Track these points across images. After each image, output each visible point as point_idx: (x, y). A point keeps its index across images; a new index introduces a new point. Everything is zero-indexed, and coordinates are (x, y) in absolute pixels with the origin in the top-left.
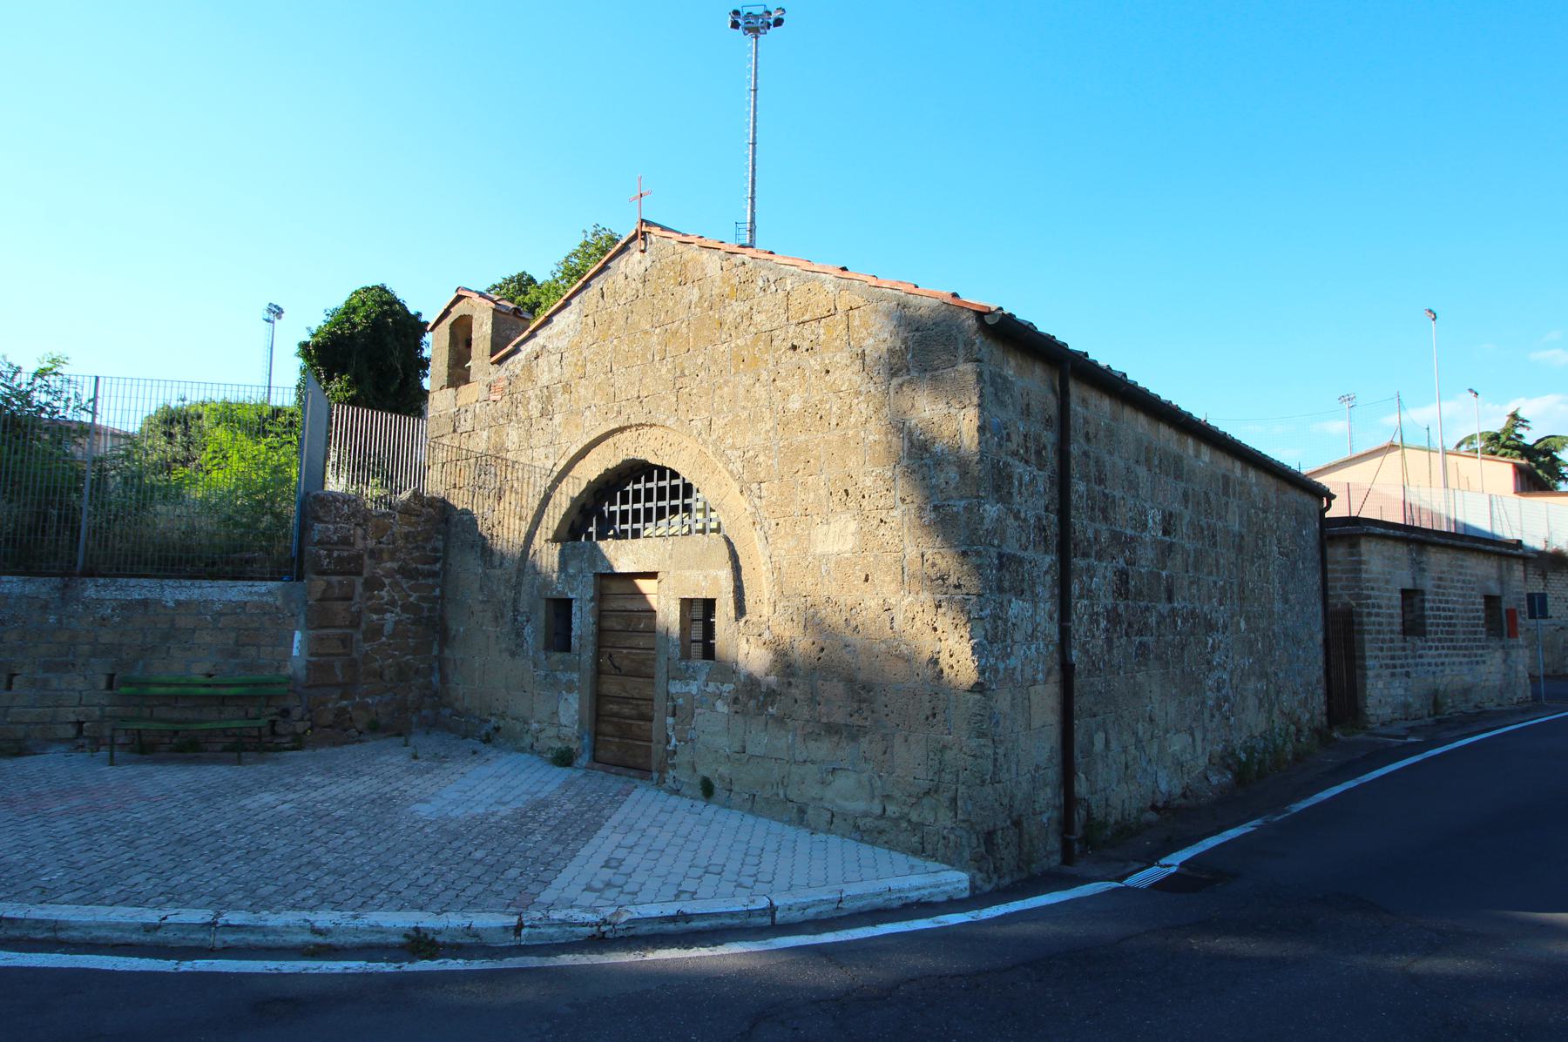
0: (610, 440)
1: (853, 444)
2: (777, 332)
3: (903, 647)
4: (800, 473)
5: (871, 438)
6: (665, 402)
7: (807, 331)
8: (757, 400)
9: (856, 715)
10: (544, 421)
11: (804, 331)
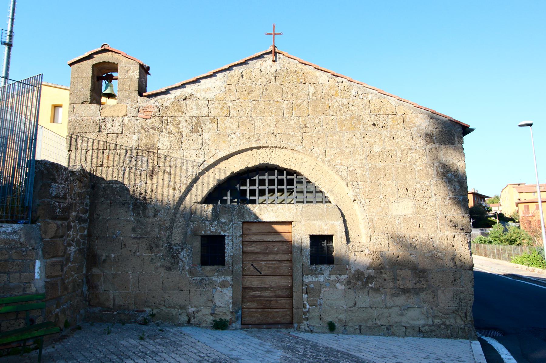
0: (249, 152)
1: (409, 170)
2: (365, 117)
3: (439, 254)
4: (382, 179)
5: (418, 168)
6: (294, 138)
7: (382, 118)
8: (355, 145)
9: (418, 283)
10: (194, 136)
11: (380, 119)
